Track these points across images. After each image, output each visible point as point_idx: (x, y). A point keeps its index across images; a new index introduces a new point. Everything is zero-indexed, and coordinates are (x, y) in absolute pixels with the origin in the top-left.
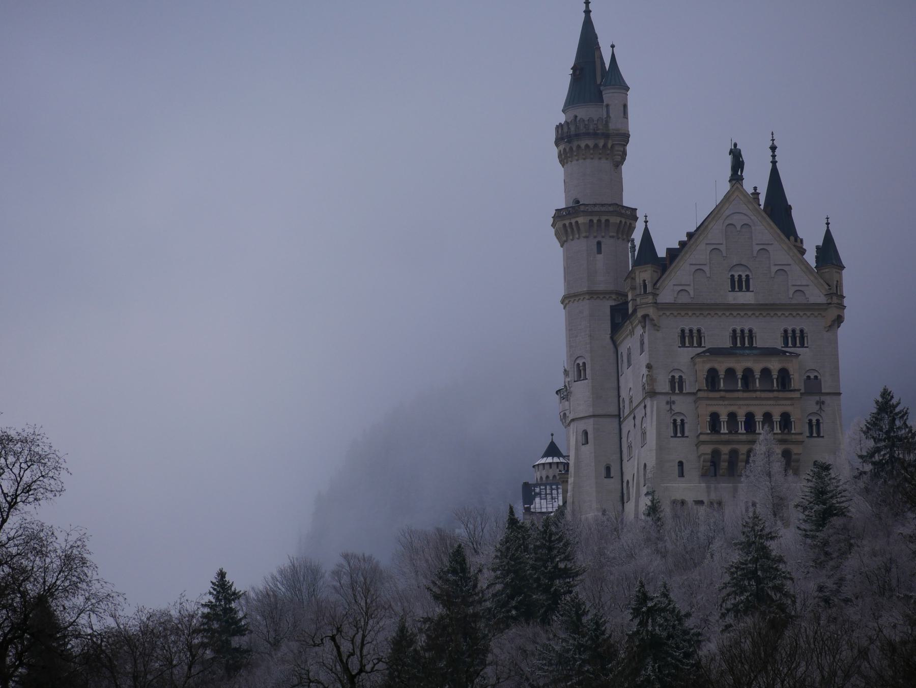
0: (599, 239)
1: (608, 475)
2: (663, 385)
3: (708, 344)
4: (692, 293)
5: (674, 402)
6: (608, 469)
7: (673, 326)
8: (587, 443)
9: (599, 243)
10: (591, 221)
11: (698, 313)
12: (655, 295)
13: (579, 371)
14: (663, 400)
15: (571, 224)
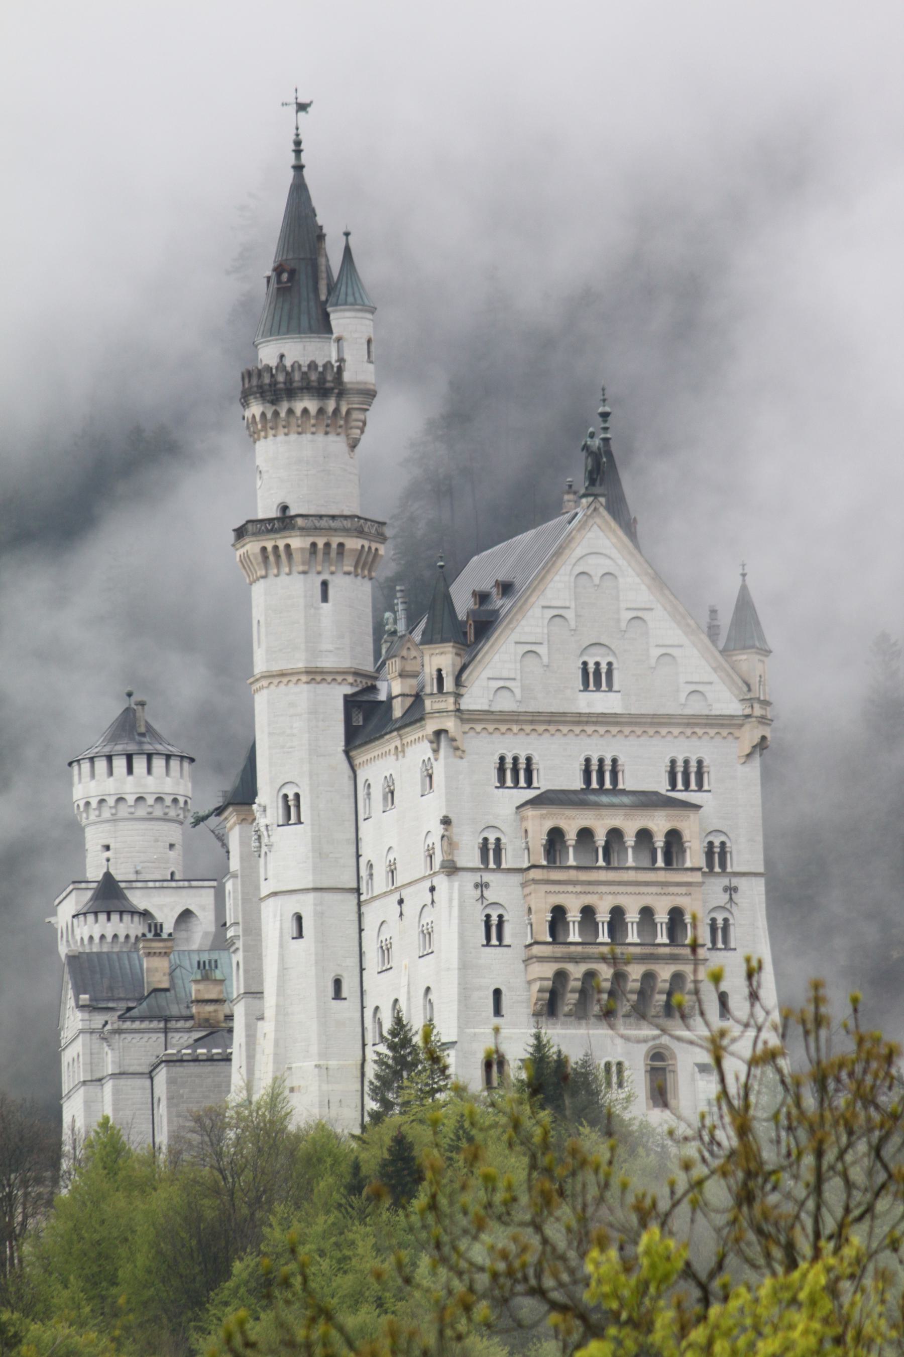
0: (325, 576)
1: (338, 995)
2: (469, 856)
3: (544, 782)
4: (517, 691)
5: (487, 885)
6: (338, 983)
7: (487, 748)
8: (300, 935)
9: (325, 584)
10: (314, 545)
11: (528, 728)
12: (458, 696)
13: (288, 808)
14: (470, 879)
15: (276, 548)
